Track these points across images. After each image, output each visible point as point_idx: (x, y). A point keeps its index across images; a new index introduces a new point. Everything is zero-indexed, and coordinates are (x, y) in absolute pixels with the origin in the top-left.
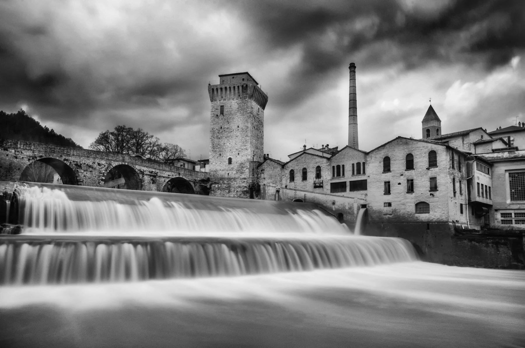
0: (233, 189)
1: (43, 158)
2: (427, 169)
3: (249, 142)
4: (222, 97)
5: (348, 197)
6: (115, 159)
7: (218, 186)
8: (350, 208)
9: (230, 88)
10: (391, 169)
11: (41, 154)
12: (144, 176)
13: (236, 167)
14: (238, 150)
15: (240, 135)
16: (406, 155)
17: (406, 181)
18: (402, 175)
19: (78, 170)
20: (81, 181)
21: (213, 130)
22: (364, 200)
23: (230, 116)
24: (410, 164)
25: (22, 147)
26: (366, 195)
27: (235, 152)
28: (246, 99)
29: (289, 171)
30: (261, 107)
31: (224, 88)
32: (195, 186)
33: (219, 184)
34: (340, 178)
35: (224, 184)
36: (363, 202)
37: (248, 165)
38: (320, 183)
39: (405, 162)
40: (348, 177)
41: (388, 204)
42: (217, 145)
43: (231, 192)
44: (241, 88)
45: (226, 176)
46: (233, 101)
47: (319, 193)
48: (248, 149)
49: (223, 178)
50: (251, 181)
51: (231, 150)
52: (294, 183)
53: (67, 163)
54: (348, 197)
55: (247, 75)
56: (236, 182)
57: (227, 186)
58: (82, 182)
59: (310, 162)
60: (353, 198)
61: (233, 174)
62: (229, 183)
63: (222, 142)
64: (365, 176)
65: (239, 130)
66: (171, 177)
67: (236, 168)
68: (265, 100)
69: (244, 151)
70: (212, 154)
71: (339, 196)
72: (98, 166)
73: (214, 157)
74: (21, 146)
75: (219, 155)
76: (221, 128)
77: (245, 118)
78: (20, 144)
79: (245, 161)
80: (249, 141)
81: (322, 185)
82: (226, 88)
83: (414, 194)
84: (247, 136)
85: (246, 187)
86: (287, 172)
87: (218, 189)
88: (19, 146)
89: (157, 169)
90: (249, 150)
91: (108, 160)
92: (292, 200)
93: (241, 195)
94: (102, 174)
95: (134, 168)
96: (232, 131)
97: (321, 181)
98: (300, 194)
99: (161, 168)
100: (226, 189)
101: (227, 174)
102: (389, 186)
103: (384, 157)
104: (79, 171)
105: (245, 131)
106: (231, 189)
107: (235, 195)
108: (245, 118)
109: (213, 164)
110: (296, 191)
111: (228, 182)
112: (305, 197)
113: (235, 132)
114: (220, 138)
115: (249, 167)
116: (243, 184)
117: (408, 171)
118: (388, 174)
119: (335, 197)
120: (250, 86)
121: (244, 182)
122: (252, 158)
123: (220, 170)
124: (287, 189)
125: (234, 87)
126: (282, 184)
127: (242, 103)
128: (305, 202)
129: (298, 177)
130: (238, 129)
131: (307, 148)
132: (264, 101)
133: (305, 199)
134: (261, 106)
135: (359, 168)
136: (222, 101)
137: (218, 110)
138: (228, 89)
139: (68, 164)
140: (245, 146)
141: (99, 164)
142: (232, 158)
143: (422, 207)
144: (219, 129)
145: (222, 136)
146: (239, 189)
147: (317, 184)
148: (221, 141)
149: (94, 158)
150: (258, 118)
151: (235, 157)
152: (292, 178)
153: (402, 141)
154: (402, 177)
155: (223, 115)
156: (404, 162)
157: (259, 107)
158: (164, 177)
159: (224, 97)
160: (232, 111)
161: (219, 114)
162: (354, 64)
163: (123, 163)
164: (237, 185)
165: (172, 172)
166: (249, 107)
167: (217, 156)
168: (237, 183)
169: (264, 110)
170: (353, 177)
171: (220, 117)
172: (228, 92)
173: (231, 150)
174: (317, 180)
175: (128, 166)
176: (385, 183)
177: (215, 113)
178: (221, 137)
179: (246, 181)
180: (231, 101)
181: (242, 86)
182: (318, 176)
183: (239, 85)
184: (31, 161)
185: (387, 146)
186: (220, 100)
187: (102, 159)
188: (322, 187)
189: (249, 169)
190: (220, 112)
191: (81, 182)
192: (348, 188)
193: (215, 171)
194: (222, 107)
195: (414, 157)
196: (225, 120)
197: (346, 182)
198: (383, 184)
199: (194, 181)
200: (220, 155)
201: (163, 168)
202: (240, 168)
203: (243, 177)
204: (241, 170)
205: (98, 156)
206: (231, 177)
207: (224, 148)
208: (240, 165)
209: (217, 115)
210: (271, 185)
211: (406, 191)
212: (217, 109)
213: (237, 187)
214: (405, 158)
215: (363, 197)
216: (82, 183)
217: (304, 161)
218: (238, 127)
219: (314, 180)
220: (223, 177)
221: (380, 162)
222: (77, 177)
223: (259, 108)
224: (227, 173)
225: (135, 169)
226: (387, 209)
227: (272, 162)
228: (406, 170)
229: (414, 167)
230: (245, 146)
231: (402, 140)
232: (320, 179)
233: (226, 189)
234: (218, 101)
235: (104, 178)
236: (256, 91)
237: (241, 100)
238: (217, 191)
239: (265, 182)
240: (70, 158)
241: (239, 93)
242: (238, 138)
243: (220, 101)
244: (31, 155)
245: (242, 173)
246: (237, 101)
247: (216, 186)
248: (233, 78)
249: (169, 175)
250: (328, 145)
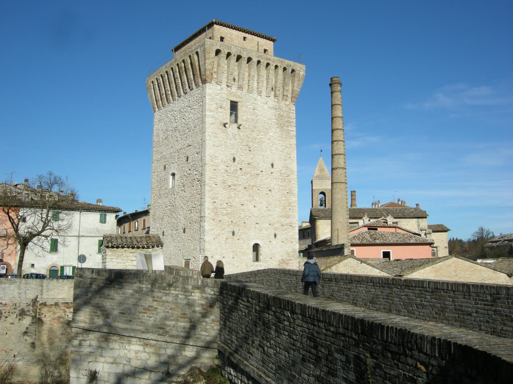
14: (273, 225)
15: (276, 187)
23: (254, 135)
27: (266, 230)
31: (246, 59)
42: (225, 205)
46: (259, 97)
48: (293, 225)
63: (237, 200)
69: (286, 229)
70: (211, 230)
73: (216, 237)
76: (234, 159)
84: (290, 193)
105: (287, 181)
113: (264, 178)
120: (301, 76)
127: (278, 110)
130: (272, 170)
137: (223, 110)
140: (288, 217)
142: (261, 245)
144: (229, 162)
145: (235, 183)
148: (233, 195)
166: (293, 122)
178: (235, 185)
183: (279, 65)
194: (234, 106)
196: (242, 142)
200: (233, 233)
207: (242, 216)
218: (272, 165)
227: (363, 264)
234: (224, 86)
237: (276, 100)
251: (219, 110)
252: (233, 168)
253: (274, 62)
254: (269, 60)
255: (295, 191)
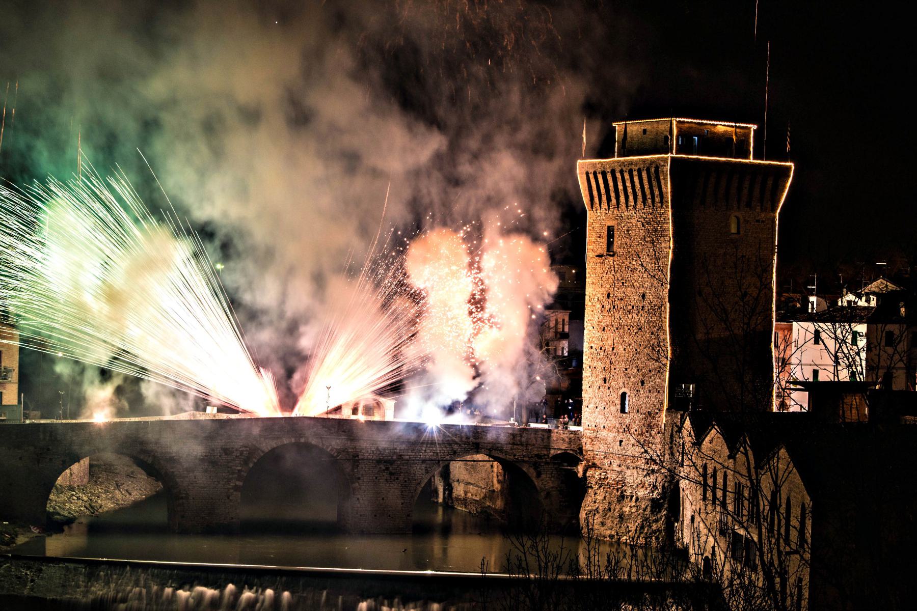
20: (181, 496)
32: (539, 475)
53: (145, 460)
72: (224, 457)
94: (233, 473)
101: (618, 443)
167: (598, 384)
204: (648, 435)
218: (643, 296)
235: (240, 483)
252: (607, 307)
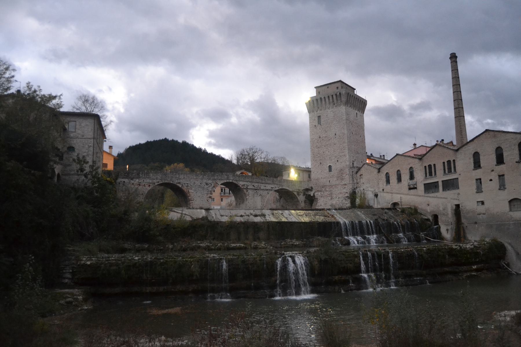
0: (335, 196)
1: (160, 183)
2: (516, 162)
3: (347, 148)
4: (319, 108)
5: (441, 198)
6: (220, 177)
7: (321, 193)
8: (444, 210)
9: (325, 98)
10: (481, 165)
11: (158, 181)
12: (248, 191)
13: (336, 173)
15: (337, 142)
16: (495, 148)
17: (498, 177)
18: (493, 171)
19: (189, 191)
21: (312, 140)
22: (457, 199)
24: (500, 160)
25: (143, 176)
26: (459, 194)
28: (341, 107)
29: (385, 175)
30: (360, 112)
31: (319, 99)
33: (321, 191)
34: (432, 179)
35: (327, 191)
36: (457, 203)
37: (347, 171)
38: (414, 184)
39: (494, 156)
40: (440, 177)
41: (481, 203)
42: (317, 154)
43: (333, 199)
44: (334, 97)
45: (328, 183)
46: (329, 110)
47: (414, 195)
49: (325, 186)
50: (351, 187)
51: (330, 158)
52: (390, 186)
53: (179, 186)
54: (441, 198)
55: (340, 83)
56: (337, 189)
57: (329, 193)
58: (194, 200)
59: (403, 163)
60: (446, 198)
61: (334, 181)
62: (331, 190)
64: (456, 174)
65: (336, 138)
66: (274, 189)
67: (336, 175)
68: (363, 104)
70: (313, 164)
71: (433, 197)
74: (142, 175)
75: (320, 164)
76: (320, 137)
77: (342, 125)
78: (142, 174)
79: (344, 167)
80: (346, 147)
81: (416, 186)
82: (321, 98)
83: (506, 190)
85: (347, 193)
86: (383, 176)
87: (321, 197)
88: (141, 176)
89: (260, 183)
90: (347, 156)
91: (215, 180)
92: (390, 203)
93: (342, 201)
95: (238, 184)
96: (330, 140)
97: (415, 183)
98: (396, 199)
99: (264, 182)
100: (329, 196)
101: (329, 182)
102: (481, 183)
103: (473, 153)
104: (189, 191)
106: (333, 195)
107: (337, 202)
108: (342, 125)
109: (315, 172)
110: (393, 194)
111: (330, 189)
112: (401, 199)
114: (320, 147)
115: (348, 172)
116: (344, 190)
117: (499, 165)
118: (479, 171)
119: (429, 198)
121: (345, 187)
122: (352, 164)
123: (322, 178)
124: (384, 192)
125: (329, 97)
126: (379, 188)
128: (401, 206)
129: (393, 179)
130: (336, 136)
131: (417, 146)
132: (363, 105)
133: (401, 202)
134: (359, 110)
135: (450, 166)
136: (318, 112)
138: (323, 100)
139: (180, 186)
141: (207, 184)
143: (516, 203)
146: (340, 196)
147: (411, 186)
148: (320, 150)
149: (202, 179)
150: (356, 123)
151: (335, 164)
152: (388, 181)
153: (490, 134)
154: (493, 173)
155: (321, 125)
156: (494, 157)
157: (356, 112)
158: (267, 190)
159: (320, 108)
160: (328, 119)
161: (317, 124)
162: (455, 54)
163: (228, 181)
164: (339, 192)
165: (274, 184)
167: (318, 165)
168: (338, 190)
169: (363, 113)
170: (444, 176)
171: (318, 128)
172: (323, 102)
173: (330, 158)
174: (411, 182)
175: (232, 183)
176: (477, 180)
177: (313, 124)
178: (321, 146)
179: (346, 186)
180: (327, 110)
181: (336, 95)
182: (412, 177)
183: (333, 94)
184: (151, 187)
185: (475, 141)
186: (317, 111)
187: (209, 179)
188: (416, 188)
189: (349, 175)
190: (317, 122)
191: (192, 200)
192: (441, 188)
193: (317, 180)
194: (319, 117)
195: (504, 150)
197: (438, 182)
198: (475, 181)
199: (297, 191)
200: (321, 163)
201: (265, 181)
202: (340, 175)
203: (343, 183)
204: (341, 177)
205: (205, 177)
206: (333, 184)
208: (340, 172)
209: (315, 126)
210: (370, 189)
211: (498, 187)
212: (314, 120)
213: (338, 194)
214: (494, 152)
215: (456, 197)
216: (193, 201)
217: (398, 163)
218: (335, 134)
219: (409, 182)
220: (325, 185)
221: (470, 159)
222: (188, 196)
223: (357, 113)
224: (329, 180)
225: (239, 185)
226: (481, 209)
227: (369, 166)
228: (496, 165)
229: (504, 161)
230: (343, 153)
231: (489, 133)
232: (413, 181)
233: (329, 196)
234: (315, 112)
236: (350, 97)
238: (320, 198)
239: (364, 187)
240: (181, 181)
241: (333, 101)
242: (336, 145)
243: (316, 111)
244: (151, 182)
245: (342, 179)
246: (332, 109)
247: (319, 194)
248: (328, 87)
249: (272, 188)
250: (443, 140)
251: (314, 121)
252: (320, 140)
253: (331, 94)
254: (329, 94)
255: (346, 141)
